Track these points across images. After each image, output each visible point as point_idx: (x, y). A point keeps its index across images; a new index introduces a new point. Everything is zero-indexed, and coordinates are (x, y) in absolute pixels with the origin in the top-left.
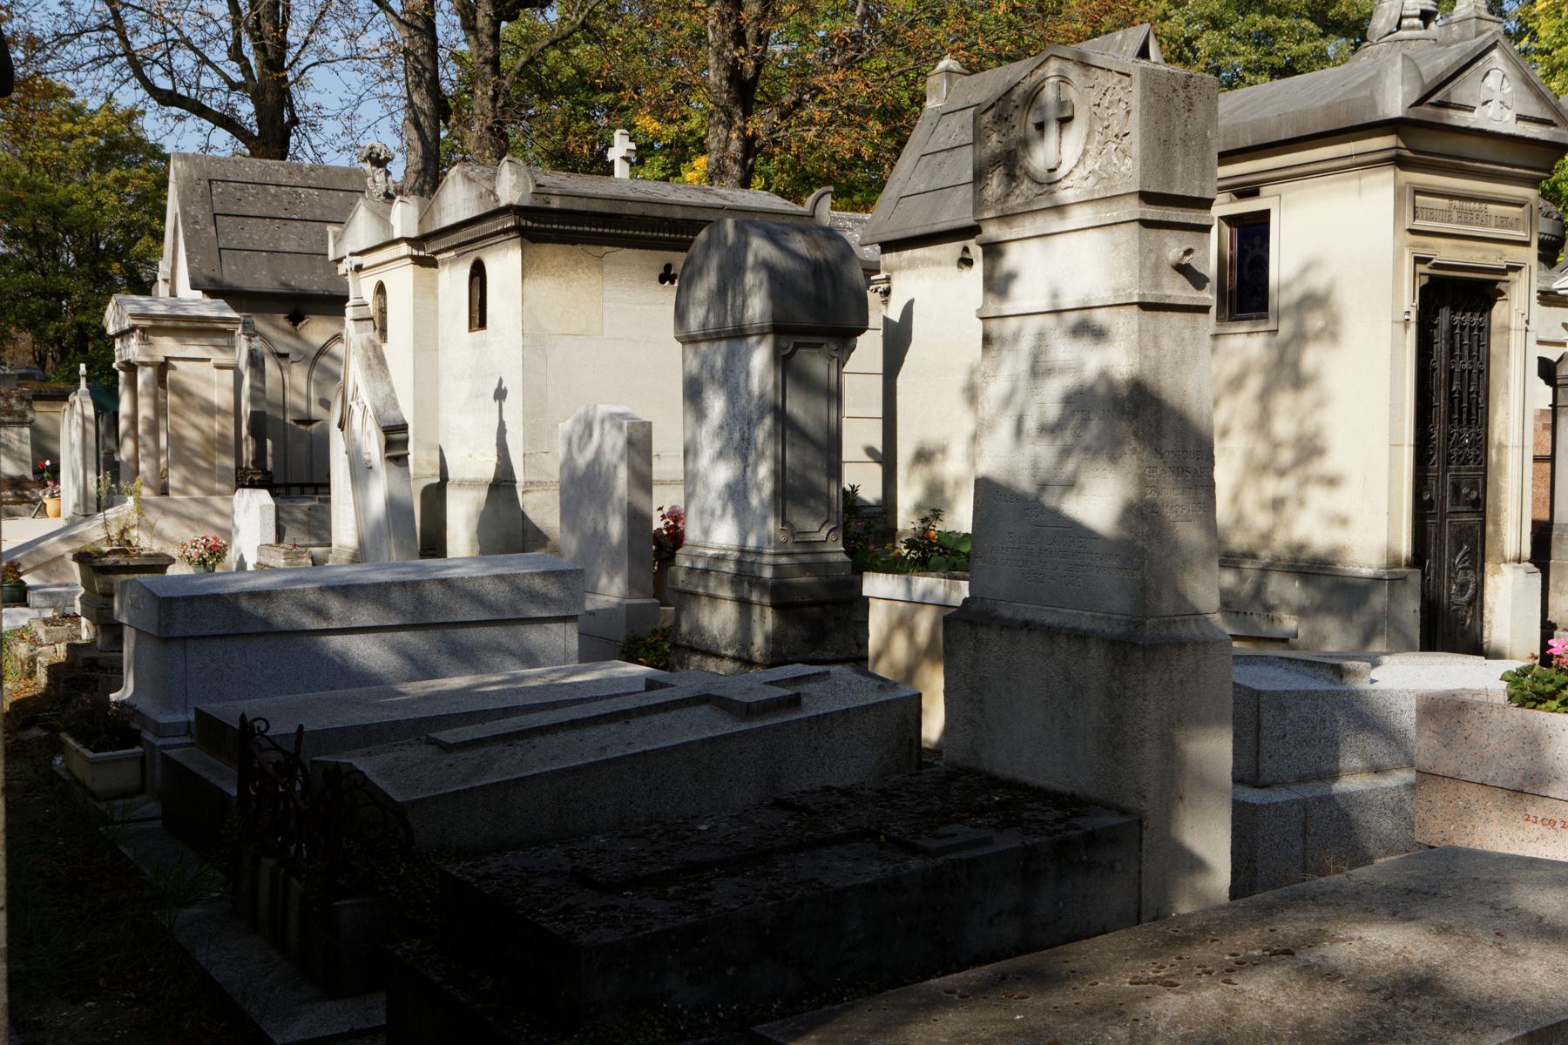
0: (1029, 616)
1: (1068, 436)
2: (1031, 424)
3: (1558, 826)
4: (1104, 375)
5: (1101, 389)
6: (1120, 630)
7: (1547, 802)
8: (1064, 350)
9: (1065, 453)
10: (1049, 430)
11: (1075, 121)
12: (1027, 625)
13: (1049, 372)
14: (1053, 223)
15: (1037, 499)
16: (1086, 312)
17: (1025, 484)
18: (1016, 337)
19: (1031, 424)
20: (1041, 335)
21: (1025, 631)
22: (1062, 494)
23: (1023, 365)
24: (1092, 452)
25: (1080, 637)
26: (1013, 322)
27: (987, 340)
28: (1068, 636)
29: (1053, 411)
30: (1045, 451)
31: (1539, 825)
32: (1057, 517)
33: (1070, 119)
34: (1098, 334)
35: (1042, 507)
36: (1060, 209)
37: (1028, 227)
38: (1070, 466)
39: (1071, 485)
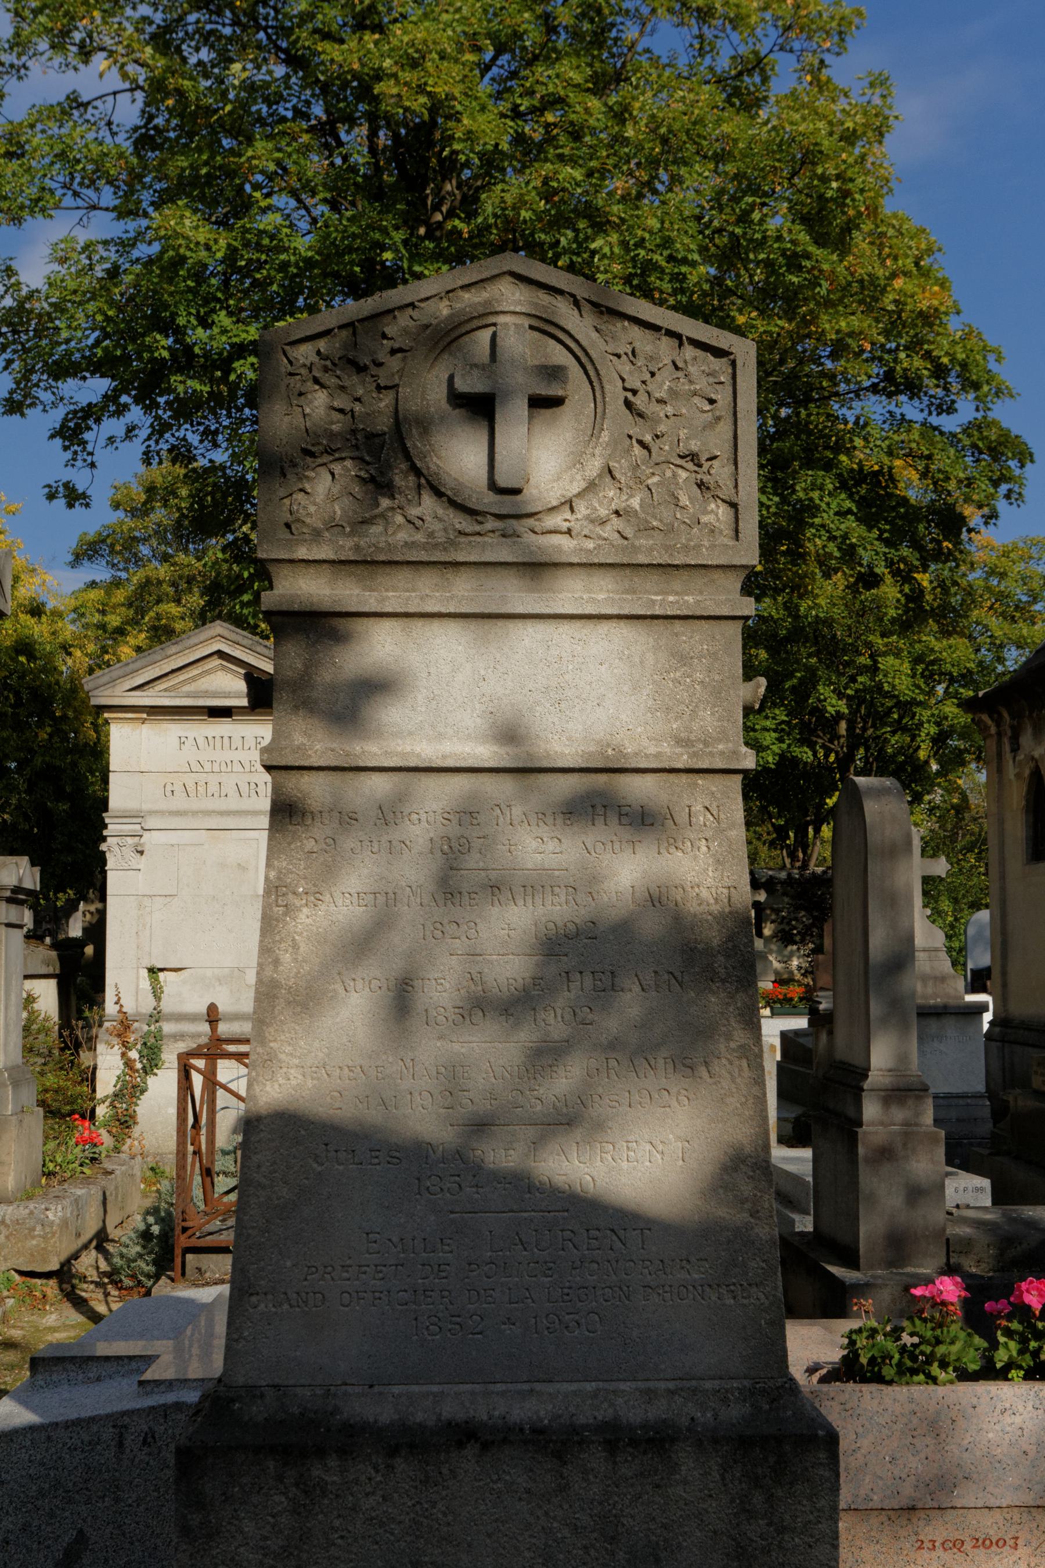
0: (449, 1410)
1: (554, 1023)
2: (441, 989)
3: (968, 1546)
4: (656, 899)
5: (651, 926)
6: (735, 1412)
7: (950, 1515)
8: (538, 847)
9: (545, 1056)
10: (481, 1005)
11: (566, 408)
12: (465, 1435)
13: (495, 888)
14: (520, 598)
15: (459, 1154)
16: (603, 778)
17: (424, 1119)
18: (388, 814)
19: (441, 989)
20: (467, 814)
21: (471, 1450)
22: (538, 1143)
23: (414, 871)
24: (635, 1051)
25: (657, 1441)
26: (379, 785)
27: (286, 813)
28: (612, 1447)
29: (510, 970)
30: (490, 1054)
31: (940, 1552)
32: (522, 1186)
33: (556, 402)
34: (643, 821)
35: (477, 1169)
36: (537, 568)
37: (394, 592)
38: (563, 1082)
39: (567, 1120)
